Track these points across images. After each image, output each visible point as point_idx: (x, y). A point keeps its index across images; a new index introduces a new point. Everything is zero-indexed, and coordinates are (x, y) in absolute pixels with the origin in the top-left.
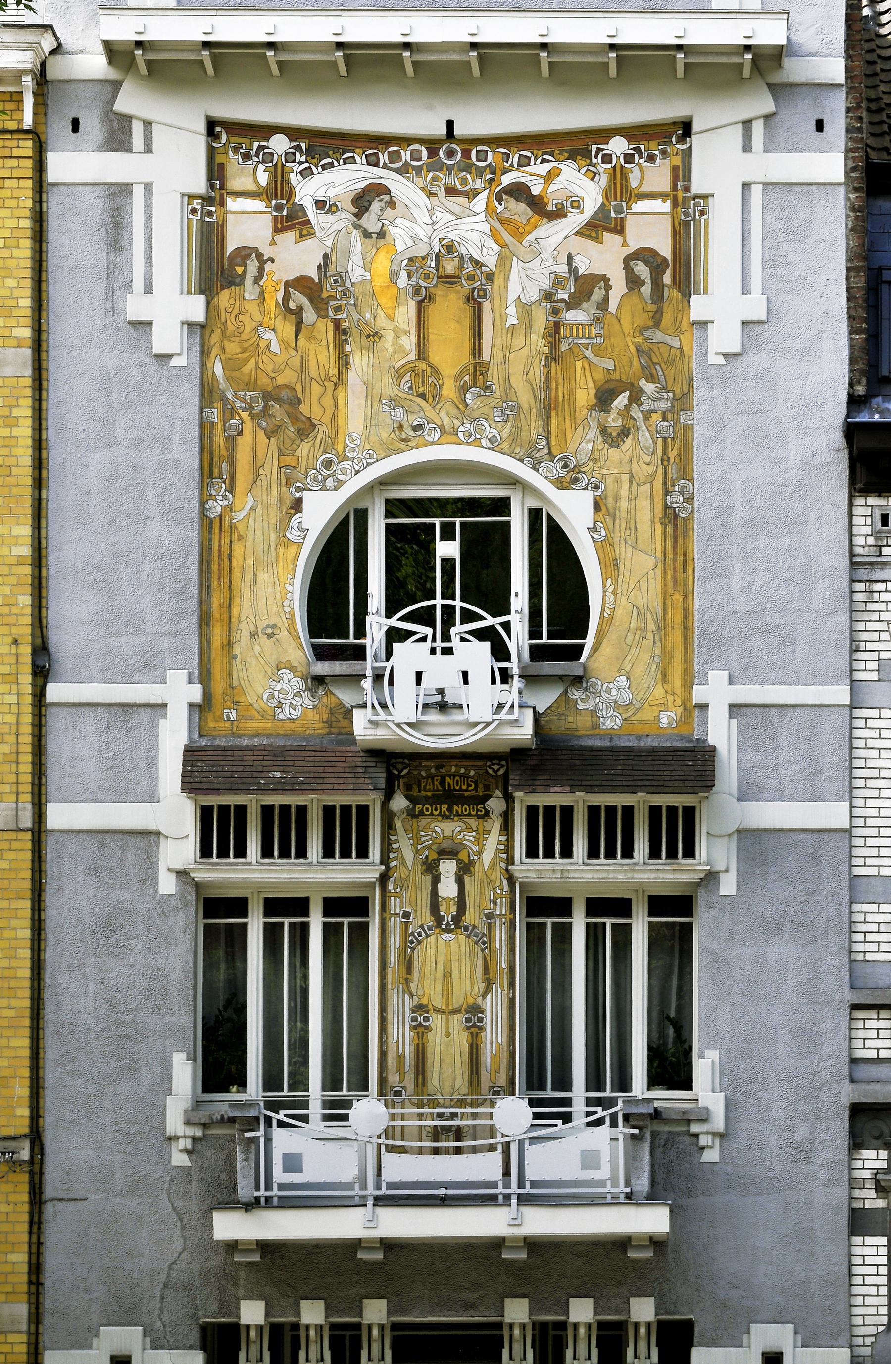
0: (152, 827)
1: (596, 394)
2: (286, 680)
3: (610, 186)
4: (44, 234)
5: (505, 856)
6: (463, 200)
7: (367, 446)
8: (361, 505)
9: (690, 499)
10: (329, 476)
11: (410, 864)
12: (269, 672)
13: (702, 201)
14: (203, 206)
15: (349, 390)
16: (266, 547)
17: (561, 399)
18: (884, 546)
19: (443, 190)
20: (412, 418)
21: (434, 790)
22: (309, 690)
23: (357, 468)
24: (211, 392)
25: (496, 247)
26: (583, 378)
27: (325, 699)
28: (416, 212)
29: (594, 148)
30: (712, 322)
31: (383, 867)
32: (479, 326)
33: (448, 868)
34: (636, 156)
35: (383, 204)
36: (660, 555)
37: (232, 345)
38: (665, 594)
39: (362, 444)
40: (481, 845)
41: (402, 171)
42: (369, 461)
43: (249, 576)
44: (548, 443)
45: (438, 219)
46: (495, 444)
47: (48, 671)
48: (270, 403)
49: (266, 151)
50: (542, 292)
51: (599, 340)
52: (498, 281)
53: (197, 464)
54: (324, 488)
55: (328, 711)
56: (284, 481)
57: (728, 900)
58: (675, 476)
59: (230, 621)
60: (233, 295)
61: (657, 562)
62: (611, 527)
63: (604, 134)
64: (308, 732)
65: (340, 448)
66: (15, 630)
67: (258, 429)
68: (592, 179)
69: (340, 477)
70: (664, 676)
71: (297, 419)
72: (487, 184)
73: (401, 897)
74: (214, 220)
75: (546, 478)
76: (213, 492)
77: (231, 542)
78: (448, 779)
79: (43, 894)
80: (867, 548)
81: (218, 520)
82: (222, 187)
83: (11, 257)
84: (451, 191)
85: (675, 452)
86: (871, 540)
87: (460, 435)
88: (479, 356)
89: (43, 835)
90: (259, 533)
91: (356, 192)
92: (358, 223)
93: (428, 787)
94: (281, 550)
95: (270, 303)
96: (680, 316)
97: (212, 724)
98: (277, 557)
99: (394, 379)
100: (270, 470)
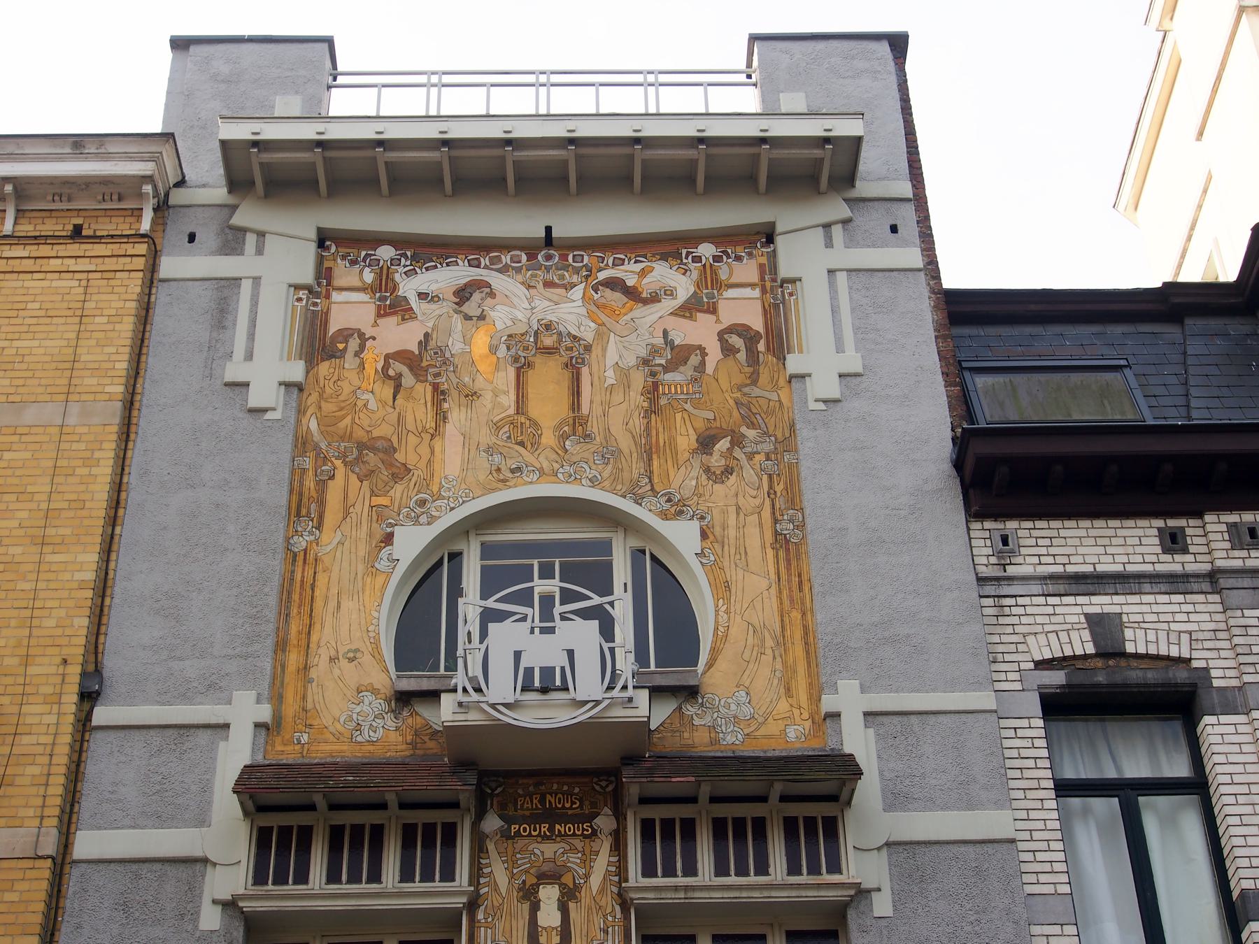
0: (198, 853)
1: (697, 440)
2: (366, 702)
3: (701, 279)
4: (149, 319)
5: (616, 879)
6: (561, 291)
7: (463, 486)
8: (456, 548)
9: (802, 526)
10: (423, 513)
11: (503, 891)
12: (349, 694)
13: (790, 286)
14: (308, 299)
15: (446, 439)
16: (353, 575)
17: (662, 444)
18: (1008, 564)
19: (541, 283)
20: (509, 462)
21: (532, 809)
22: (393, 711)
23: (452, 505)
24: (304, 443)
25: (592, 325)
26: (683, 426)
27: (410, 721)
28: (515, 300)
29: (684, 252)
30: (809, 375)
31: (472, 889)
32: (578, 387)
33: (549, 895)
34: (725, 257)
35: (484, 295)
36: (773, 576)
37: (330, 405)
38: (782, 612)
39: (458, 485)
40: (588, 867)
41: (504, 270)
42: (464, 499)
43: (332, 604)
44: (650, 481)
45: (537, 305)
46: (596, 483)
47: (98, 693)
48: (364, 452)
49: (372, 258)
50: (639, 359)
51: (697, 395)
52: (596, 351)
53: (284, 502)
54: (416, 522)
55: (413, 732)
56: (375, 518)
57: (883, 923)
58: (783, 507)
59: (308, 646)
60: (333, 365)
61: (771, 583)
62: (720, 553)
63: (693, 238)
64: (389, 754)
65: (435, 489)
66: (65, 651)
67: (350, 473)
68: (684, 274)
69: (433, 513)
70: (788, 690)
71: (392, 465)
72: (584, 279)
73: (493, 927)
74: (319, 308)
75: (650, 510)
76: (299, 529)
77: (315, 573)
78: (548, 797)
79: (57, 934)
80: (990, 567)
81: (302, 554)
82: (329, 284)
83: (114, 330)
84: (548, 284)
85: (781, 486)
86: (993, 560)
87: (560, 476)
88: (578, 411)
89: (67, 869)
90: (345, 564)
91: (458, 286)
92: (460, 309)
93: (526, 806)
94: (369, 580)
95: (370, 370)
96: (776, 376)
97: (279, 748)
98: (364, 585)
99: (493, 431)
100: (361, 510)
